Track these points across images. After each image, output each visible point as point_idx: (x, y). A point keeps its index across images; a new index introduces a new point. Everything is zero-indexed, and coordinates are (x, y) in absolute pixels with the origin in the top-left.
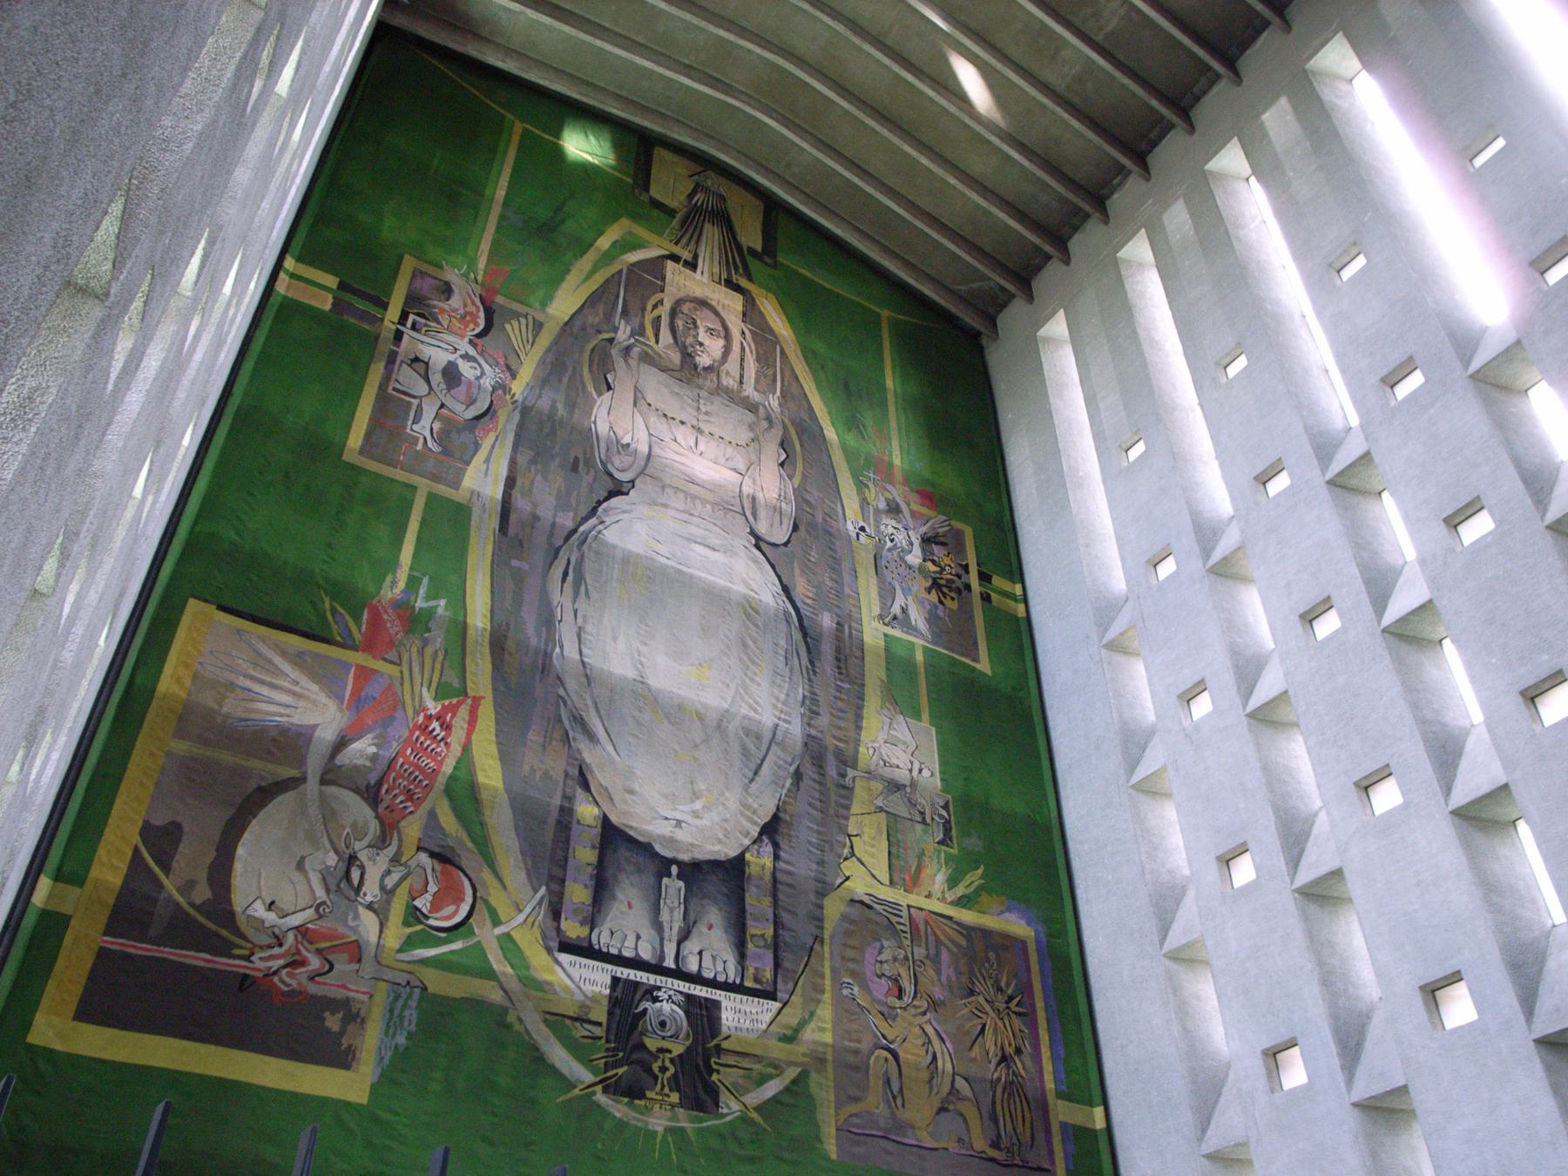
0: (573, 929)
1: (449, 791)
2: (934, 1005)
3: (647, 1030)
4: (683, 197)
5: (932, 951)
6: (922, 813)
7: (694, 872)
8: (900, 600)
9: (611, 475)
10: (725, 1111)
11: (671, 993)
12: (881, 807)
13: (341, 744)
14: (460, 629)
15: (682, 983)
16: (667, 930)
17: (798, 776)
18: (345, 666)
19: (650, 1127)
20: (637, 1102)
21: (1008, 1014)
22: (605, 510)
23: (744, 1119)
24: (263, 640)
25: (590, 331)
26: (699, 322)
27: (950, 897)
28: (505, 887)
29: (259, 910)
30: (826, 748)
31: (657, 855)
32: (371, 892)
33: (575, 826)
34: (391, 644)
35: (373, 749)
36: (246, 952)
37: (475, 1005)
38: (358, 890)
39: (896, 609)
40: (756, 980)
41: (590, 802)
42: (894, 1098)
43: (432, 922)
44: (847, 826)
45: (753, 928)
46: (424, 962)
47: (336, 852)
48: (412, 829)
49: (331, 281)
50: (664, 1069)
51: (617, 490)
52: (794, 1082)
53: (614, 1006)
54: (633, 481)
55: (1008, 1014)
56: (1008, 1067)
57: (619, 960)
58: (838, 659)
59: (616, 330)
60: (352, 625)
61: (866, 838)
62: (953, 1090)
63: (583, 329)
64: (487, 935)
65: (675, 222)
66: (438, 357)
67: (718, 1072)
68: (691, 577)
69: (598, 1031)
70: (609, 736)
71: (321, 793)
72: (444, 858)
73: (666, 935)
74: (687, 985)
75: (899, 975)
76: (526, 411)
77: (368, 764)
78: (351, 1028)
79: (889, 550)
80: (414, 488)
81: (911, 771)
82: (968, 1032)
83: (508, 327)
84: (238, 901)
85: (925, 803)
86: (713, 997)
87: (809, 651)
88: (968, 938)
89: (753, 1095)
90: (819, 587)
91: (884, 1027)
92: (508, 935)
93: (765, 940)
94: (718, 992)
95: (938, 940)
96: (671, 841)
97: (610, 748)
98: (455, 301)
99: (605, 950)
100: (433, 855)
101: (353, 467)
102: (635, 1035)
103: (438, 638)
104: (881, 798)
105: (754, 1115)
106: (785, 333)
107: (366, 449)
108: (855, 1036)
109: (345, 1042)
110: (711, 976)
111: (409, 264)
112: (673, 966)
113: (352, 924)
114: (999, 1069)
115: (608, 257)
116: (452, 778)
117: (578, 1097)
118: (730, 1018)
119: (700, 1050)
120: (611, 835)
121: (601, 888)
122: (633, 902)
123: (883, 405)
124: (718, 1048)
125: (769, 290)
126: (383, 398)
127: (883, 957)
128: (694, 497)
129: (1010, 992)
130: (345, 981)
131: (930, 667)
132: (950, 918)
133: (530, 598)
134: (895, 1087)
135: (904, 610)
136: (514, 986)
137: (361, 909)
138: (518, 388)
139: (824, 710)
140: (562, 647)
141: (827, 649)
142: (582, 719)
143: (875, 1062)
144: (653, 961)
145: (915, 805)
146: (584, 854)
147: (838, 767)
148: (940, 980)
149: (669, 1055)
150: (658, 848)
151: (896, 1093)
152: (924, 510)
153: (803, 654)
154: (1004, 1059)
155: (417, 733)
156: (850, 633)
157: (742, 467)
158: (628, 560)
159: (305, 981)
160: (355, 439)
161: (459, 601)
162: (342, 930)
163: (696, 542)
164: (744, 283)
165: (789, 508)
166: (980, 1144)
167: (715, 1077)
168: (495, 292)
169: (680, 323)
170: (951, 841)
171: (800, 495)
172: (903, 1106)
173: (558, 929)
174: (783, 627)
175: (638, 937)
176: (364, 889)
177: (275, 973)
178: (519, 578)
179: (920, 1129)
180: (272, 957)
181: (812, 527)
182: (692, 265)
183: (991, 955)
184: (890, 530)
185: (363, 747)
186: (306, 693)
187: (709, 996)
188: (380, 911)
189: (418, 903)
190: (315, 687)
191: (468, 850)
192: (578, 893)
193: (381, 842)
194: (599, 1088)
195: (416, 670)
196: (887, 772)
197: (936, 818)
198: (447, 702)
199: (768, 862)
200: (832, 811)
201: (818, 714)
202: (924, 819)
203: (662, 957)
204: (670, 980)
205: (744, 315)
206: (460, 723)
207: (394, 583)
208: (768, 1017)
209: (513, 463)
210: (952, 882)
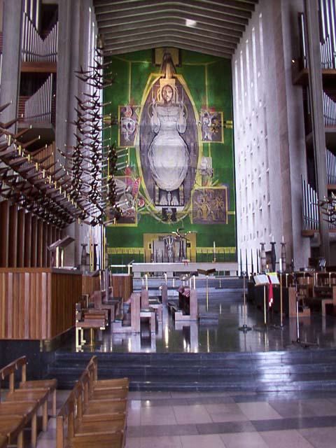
0: (157, 203)
2: (208, 202)
7: (171, 192)
23: (180, 221)
37: (147, 214)
48: (136, 196)
51: (156, 134)
64: (147, 206)
66: (126, 123)
72: (141, 198)
76: (141, 127)
90: (191, 139)
98: (127, 111)
107: (121, 145)
111: (119, 107)
115: (150, 85)
121: (160, 198)
125: (180, 74)
126: (121, 135)
130: (133, 215)
131: (211, 147)
138: (138, 123)
141: (192, 150)
146: (157, 194)
154: (219, 207)
158: (159, 147)
161: (137, 164)
164: (175, 75)
166: (214, 219)
178: (144, 156)
182: (165, 77)
185: (129, 188)
188: (135, 207)
192: (157, 199)
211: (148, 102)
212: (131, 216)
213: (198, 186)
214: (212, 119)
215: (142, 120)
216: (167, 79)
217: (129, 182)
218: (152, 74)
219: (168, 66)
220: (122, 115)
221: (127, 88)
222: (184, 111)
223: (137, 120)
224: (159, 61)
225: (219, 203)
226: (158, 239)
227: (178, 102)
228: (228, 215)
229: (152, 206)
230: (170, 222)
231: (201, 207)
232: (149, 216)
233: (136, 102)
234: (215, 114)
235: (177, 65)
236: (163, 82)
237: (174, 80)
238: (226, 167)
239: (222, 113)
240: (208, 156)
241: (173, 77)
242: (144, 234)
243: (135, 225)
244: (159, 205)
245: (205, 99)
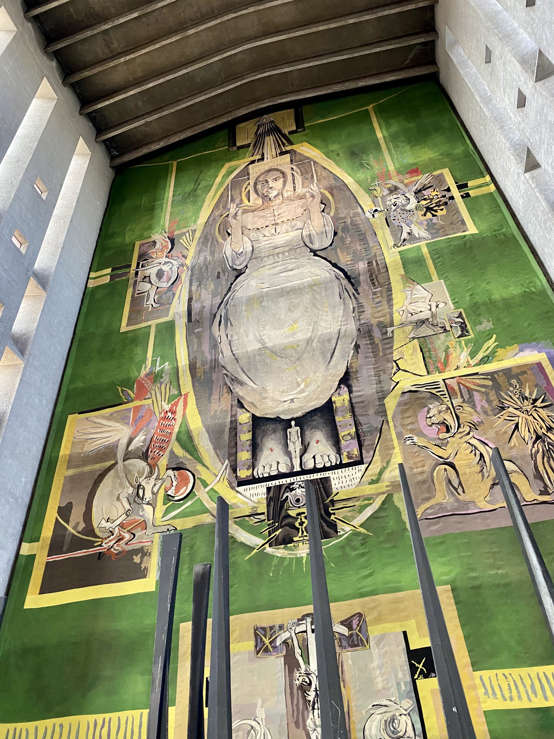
0: (243, 474)
1: (178, 439)
2: (474, 426)
3: (289, 507)
4: (252, 136)
5: (466, 396)
6: (444, 328)
8: (406, 229)
9: (236, 270)
10: (342, 533)
11: (300, 483)
12: (413, 337)
15: (305, 476)
16: (293, 453)
17: (357, 347)
18: (129, 410)
19: (299, 556)
20: (288, 545)
21: (535, 410)
22: (236, 285)
23: (356, 534)
24: (96, 417)
25: (217, 218)
26: (269, 180)
27: (472, 362)
28: (208, 469)
29: (104, 524)
30: (372, 325)
31: (283, 420)
32: (148, 496)
33: (239, 427)
35: (144, 437)
36: (100, 543)
38: (142, 499)
39: (405, 235)
40: (349, 457)
41: (245, 413)
42: (456, 489)
43: (176, 498)
44: (393, 357)
46: (174, 518)
47: (132, 486)
48: (163, 462)
50: (301, 524)
51: (239, 273)
52: (383, 503)
53: (270, 502)
54: (247, 266)
55: (535, 410)
56: (544, 442)
57: (271, 478)
58: (372, 280)
59: (229, 210)
60: (130, 392)
61: (405, 357)
63: (214, 220)
64: (202, 494)
67: (334, 514)
68: (282, 288)
69: (262, 517)
70: (250, 379)
71: (124, 465)
73: (293, 456)
74: (309, 476)
75: (445, 420)
77: (142, 444)
78: (145, 558)
79: (394, 211)
81: (430, 310)
82: (505, 432)
83: (181, 241)
85: (444, 321)
86: (326, 476)
87: (353, 285)
88: (493, 379)
89: (358, 519)
91: (440, 452)
92: (212, 489)
93: (351, 436)
94: (327, 472)
95: (469, 390)
96: (290, 410)
97: (251, 384)
98: (158, 246)
99: (261, 476)
100: (174, 469)
102: (284, 510)
103: (166, 379)
104: (412, 332)
105: (361, 530)
106: (315, 154)
108: (420, 464)
109: (143, 566)
110: (322, 466)
111: (138, 244)
112: (299, 469)
113: (141, 514)
114: (536, 445)
116: (179, 433)
117: (256, 553)
118: (337, 484)
119: (322, 506)
122: (273, 448)
123: (378, 146)
124: (333, 502)
127: (431, 414)
128: (278, 254)
129: (534, 397)
132: (476, 374)
134: (456, 484)
137: (145, 506)
140: (222, 353)
142: (236, 378)
143: (437, 474)
144: (288, 472)
145: (437, 325)
146: (245, 437)
147: (381, 331)
148: (476, 411)
149: (303, 515)
150: (283, 417)
151: (457, 487)
153: (349, 287)
155: (162, 421)
156: (377, 264)
159: (124, 546)
162: (138, 518)
163: (282, 272)
167: (333, 517)
168: (174, 231)
170: (467, 332)
171: (335, 219)
172: (464, 492)
173: (236, 477)
174: (337, 282)
175: (278, 463)
176: (145, 497)
177: (112, 547)
178: (199, 336)
179: (480, 501)
180: (110, 541)
181: (345, 229)
183: (514, 382)
184: (393, 201)
186: (114, 428)
187: (322, 476)
189: (169, 493)
190: (118, 424)
191: (190, 460)
192: (244, 456)
193: (151, 473)
194: (268, 544)
195: (158, 395)
196: (416, 318)
197: (454, 325)
198: (173, 403)
199: (346, 396)
200: (381, 354)
201: (364, 311)
202: (445, 329)
203: (293, 467)
204: (298, 477)
207: (146, 367)
208: (360, 474)
209: (190, 292)
210: (473, 354)
212: (135, 545)
214: (418, 192)
219: (270, 141)
227: (300, 190)
235: (291, 133)
240: (429, 279)
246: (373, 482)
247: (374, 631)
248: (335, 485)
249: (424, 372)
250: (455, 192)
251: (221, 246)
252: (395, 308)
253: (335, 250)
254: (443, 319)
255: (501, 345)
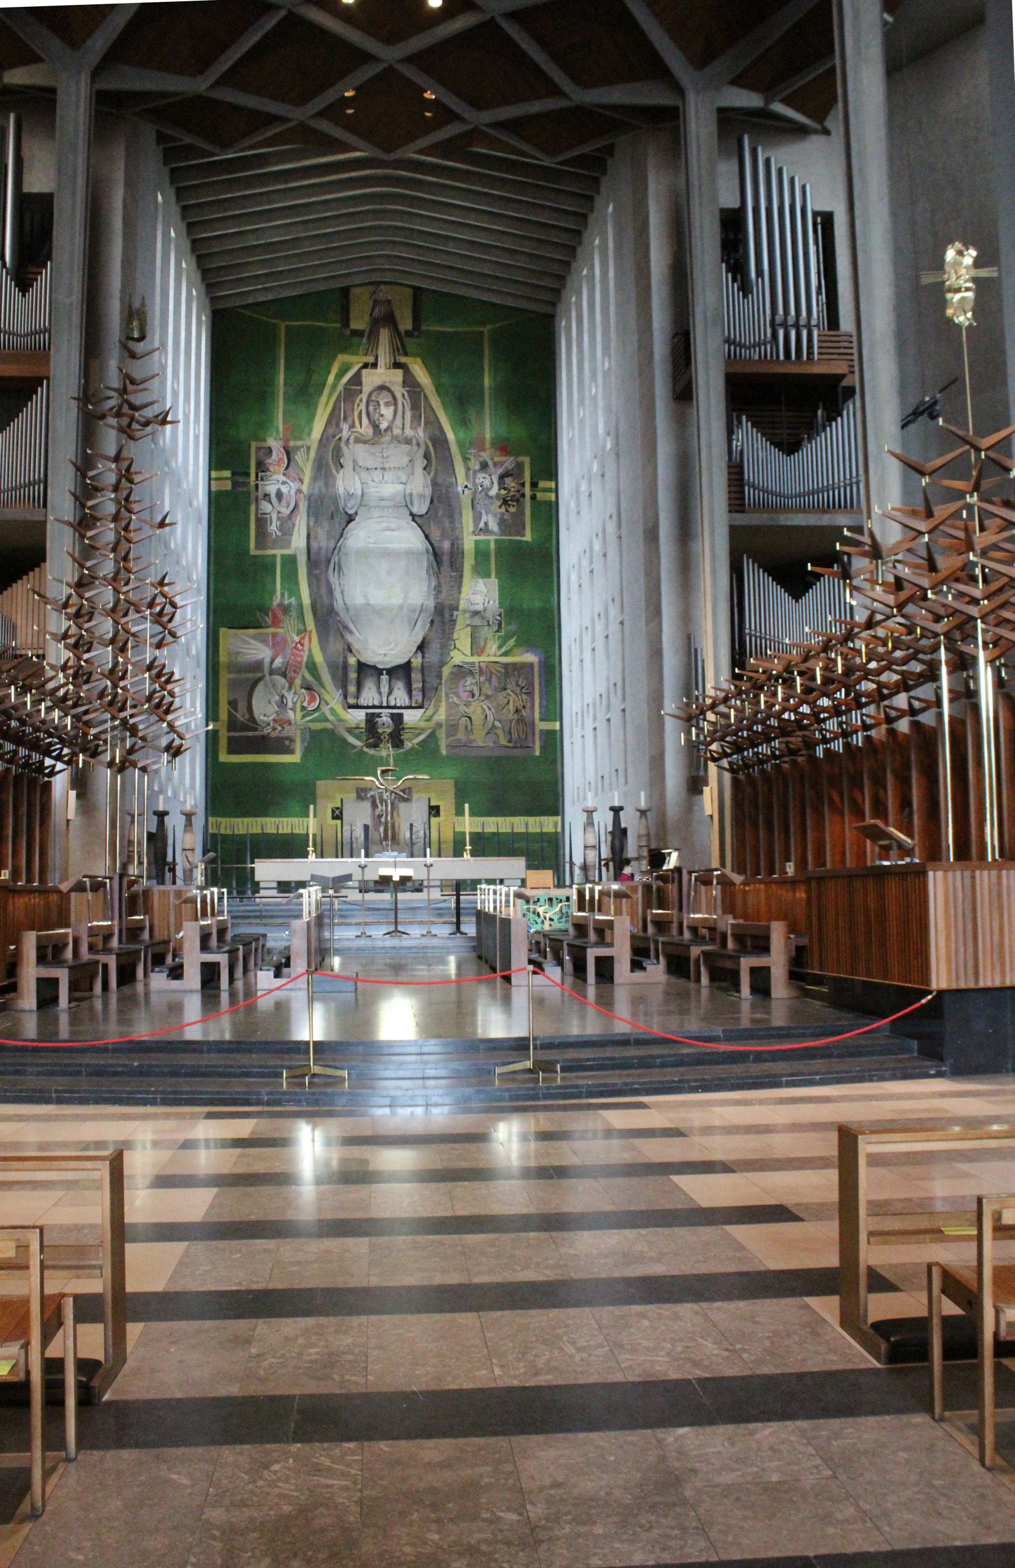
0: (351, 701)
1: (307, 667)
2: (488, 697)
4: (367, 318)
7: (391, 672)
8: (484, 518)
13: (272, 661)
14: (300, 606)
17: (432, 622)
18: (267, 634)
23: (413, 748)
29: (262, 717)
32: (290, 705)
34: (281, 621)
39: (482, 525)
45: (414, 686)
48: (298, 682)
49: (227, 474)
51: (351, 519)
62: (494, 727)
64: (325, 709)
65: (364, 340)
66: (272, 489)
72: (309, 688)
76: (309, 498)
80: (275, 556)
84: (256, 716)
95: (491, 673)
96: (383, 663)
98: (274, 456)
101: (254, 557)
103: (294, 613)
107: (257, 548)
111: (254, 445)
115: (334, 386)
120: (362, 667)
123: (482, 401)
130: (289, 731)
133: (323, 585)
135: (486, 524)
136: (335, 722)
138: (305, 488)
139: (444, 590)
141: (446, 559)
146: (353, 675)
150: (380, 667)
152: (502, 459)
154: (517, 711)
157: (404, 479)
160: (252, 544)
161: (299, 597)
164: (403, 359)
165: (428, 492)
166: (503, 741)
169: (371, 408)
171: (434, 484)
178: (317, 578)
182: (375, 365)
188: (293, 709)
192: (352, 689)
193: (290, 688)
196: (473, 608)
199: (420, 660)
205: (404, 382)
206: (306, 642)
210: (500, 647)
211: (331, 431)
212: (284, 734)
213: (461, 654)
214: (502, 478)
215: (314, 479)
216: (381, 370)
217: (278, 644)
218: (341, 358)
219: (385, 335)
220: (261, 467)
221: (273, 395)
222: (427, 456)
223: (301, 481)
224: (359, 322)
225: (514, 700)
226: (354, 795)
227: (409, 432)
228: (541, 731)
229: (339, 709)
230: (387, 751)
231: (470, 710)
232: (332, 734)
233: (296, 430)
234: (509, 462)
235: (408, 333)
236: (371, 379)
237: (399, 372)
238: (537, 604)
239: (526, 460)
241: (397, 365)
242: (318, 782)
243: (295, 758)
244: (357, 707)
245: (483, 423)
246: (427, 721)
247: (415, 797)
248: (406, 718)
249: (468, 652)
250: (527, 491)
251: (335, 479)
252: (463, 595)
253: (429, 519)
254: (489, 615)
255: (517, 645)
